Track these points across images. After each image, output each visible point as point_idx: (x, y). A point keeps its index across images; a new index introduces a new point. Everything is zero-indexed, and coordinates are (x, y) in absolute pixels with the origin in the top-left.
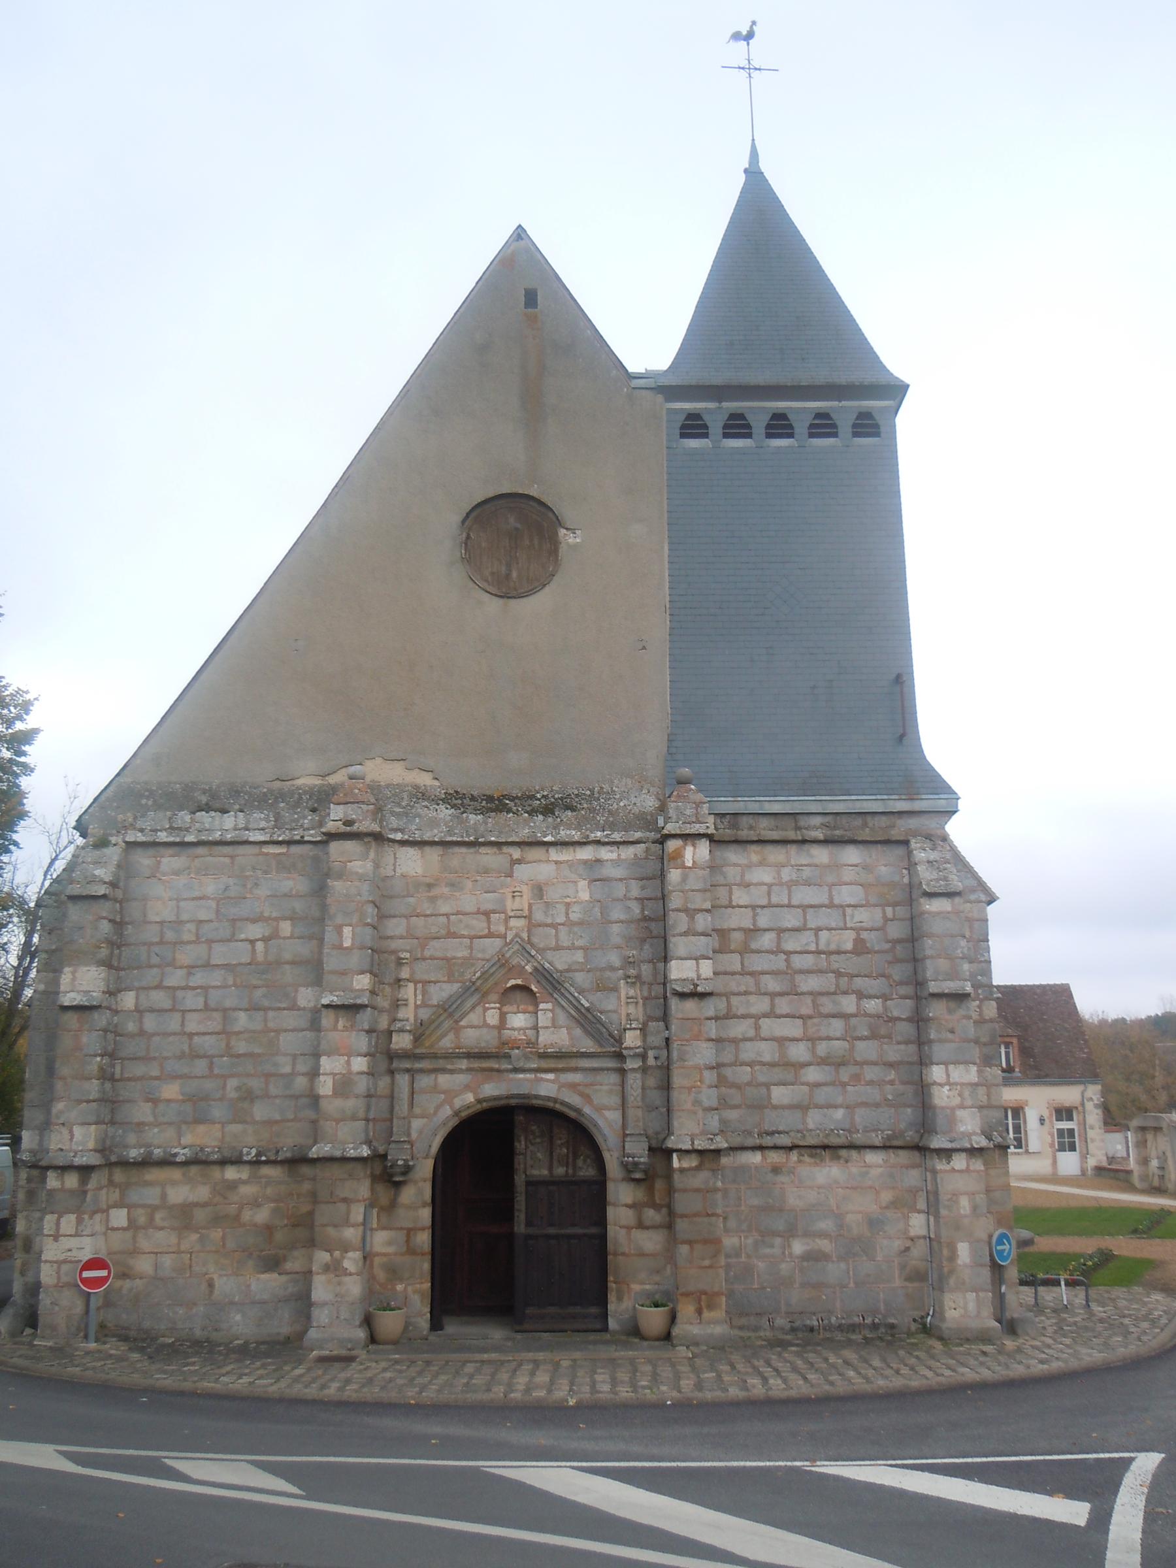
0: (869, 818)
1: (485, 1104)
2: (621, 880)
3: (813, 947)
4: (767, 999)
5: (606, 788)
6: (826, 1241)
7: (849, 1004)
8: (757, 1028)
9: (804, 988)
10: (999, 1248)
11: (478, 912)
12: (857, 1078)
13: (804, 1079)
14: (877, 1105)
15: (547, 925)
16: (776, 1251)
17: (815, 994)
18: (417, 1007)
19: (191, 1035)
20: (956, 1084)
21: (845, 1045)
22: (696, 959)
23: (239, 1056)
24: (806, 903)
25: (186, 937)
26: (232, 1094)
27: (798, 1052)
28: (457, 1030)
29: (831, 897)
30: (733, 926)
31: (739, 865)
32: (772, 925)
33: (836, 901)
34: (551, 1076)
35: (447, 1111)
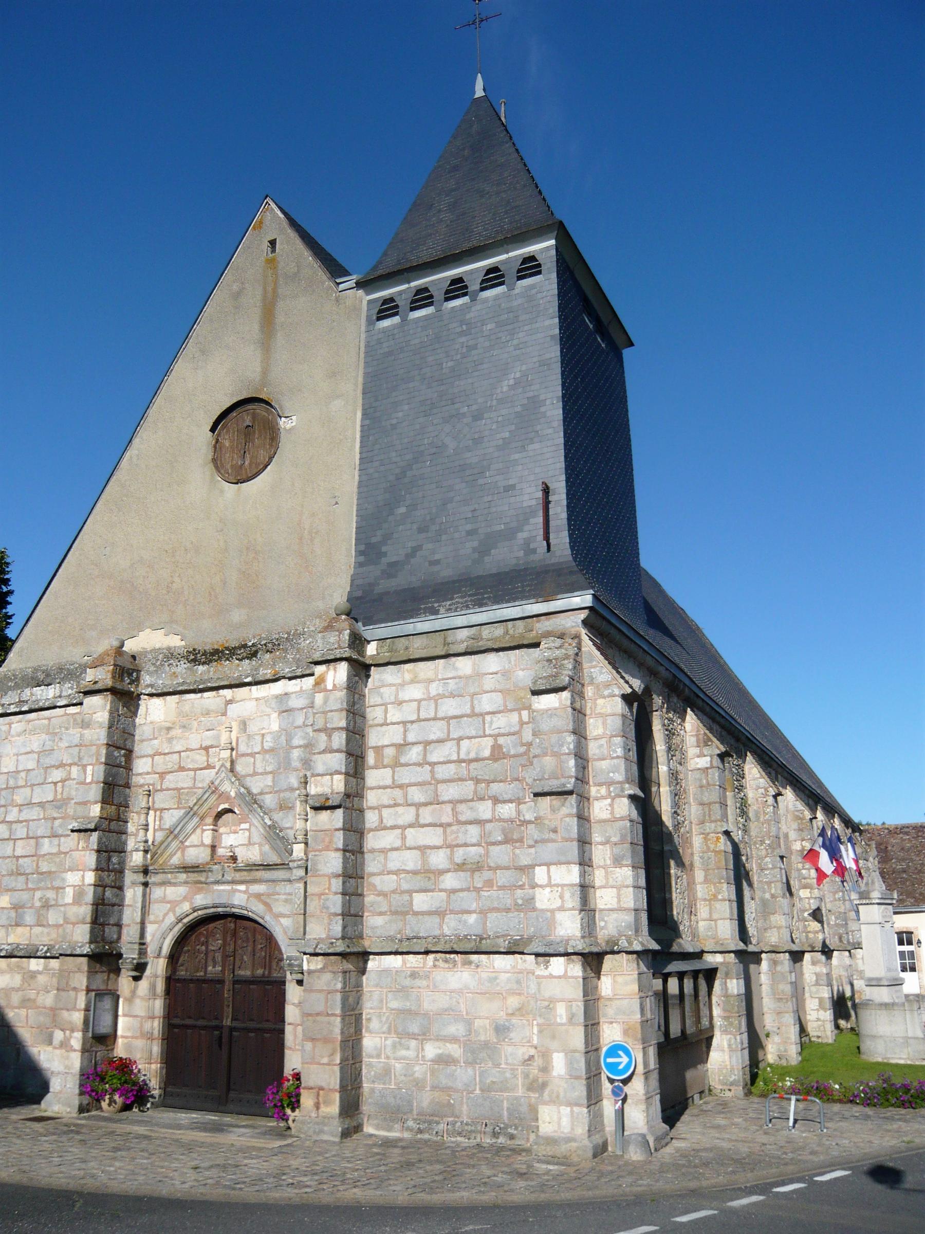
0: (510, 624)
1: (200, 913)
2: (302, 709)
3: (454, 757)
4: (412, 810)
5: (300, 629)
6: (456, 1046)
7: (484, 810)
8: (404, 838)
9: (445, 797)
10: (609, 1060)
11: (201, 748)
12: (489, 883)
13: (442, 886)
14: (508, 910)
15: (248, 755)
16: (411, 1054)
17: (454, 802)
18: (155, 830)
19: (18, 857)
20: (557, 885)
21: (480, 850)
22: (331, 774)
23: (42, 874)
24: (450, 714)
25: (21, 783)
26: (38, 904)
27: (438, 859)
28: (183, 848)
29: (473, 707)
30: (386, 743)
31: (394, 685)
32: (420, 739)
33: (477, 710)
34: (242, 887)
35: (171, 919)
